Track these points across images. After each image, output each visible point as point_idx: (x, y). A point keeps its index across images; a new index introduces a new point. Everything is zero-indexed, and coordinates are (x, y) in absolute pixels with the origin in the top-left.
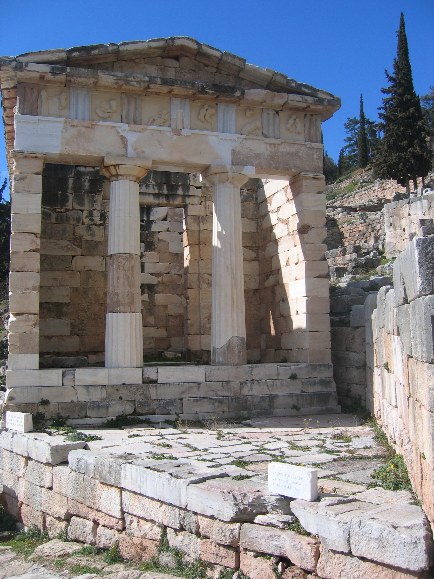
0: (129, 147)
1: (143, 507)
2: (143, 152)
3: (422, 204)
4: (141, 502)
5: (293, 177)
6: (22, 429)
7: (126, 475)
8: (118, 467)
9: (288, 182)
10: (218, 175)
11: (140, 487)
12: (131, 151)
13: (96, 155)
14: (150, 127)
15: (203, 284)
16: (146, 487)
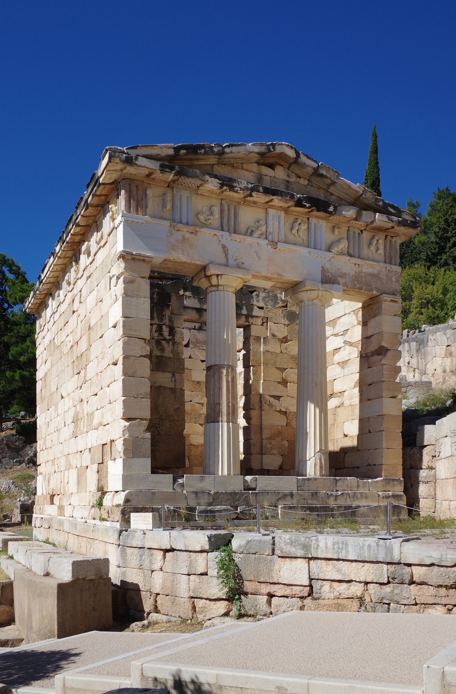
0: (230, 257)
1: (339, 571)
2: (243, 263)
3: (410, 346)
4: (337, 567)
5: (370, 299)
6: (151, 527)
7: (318, 546)
8: (307, 540)
9: (360, 305)
10: (309, 292)
11: (338, 553)
12: (231, 261)
13: (199, 263)
14: (249, 240)
15: (264, 405)
16: (347, 552)
